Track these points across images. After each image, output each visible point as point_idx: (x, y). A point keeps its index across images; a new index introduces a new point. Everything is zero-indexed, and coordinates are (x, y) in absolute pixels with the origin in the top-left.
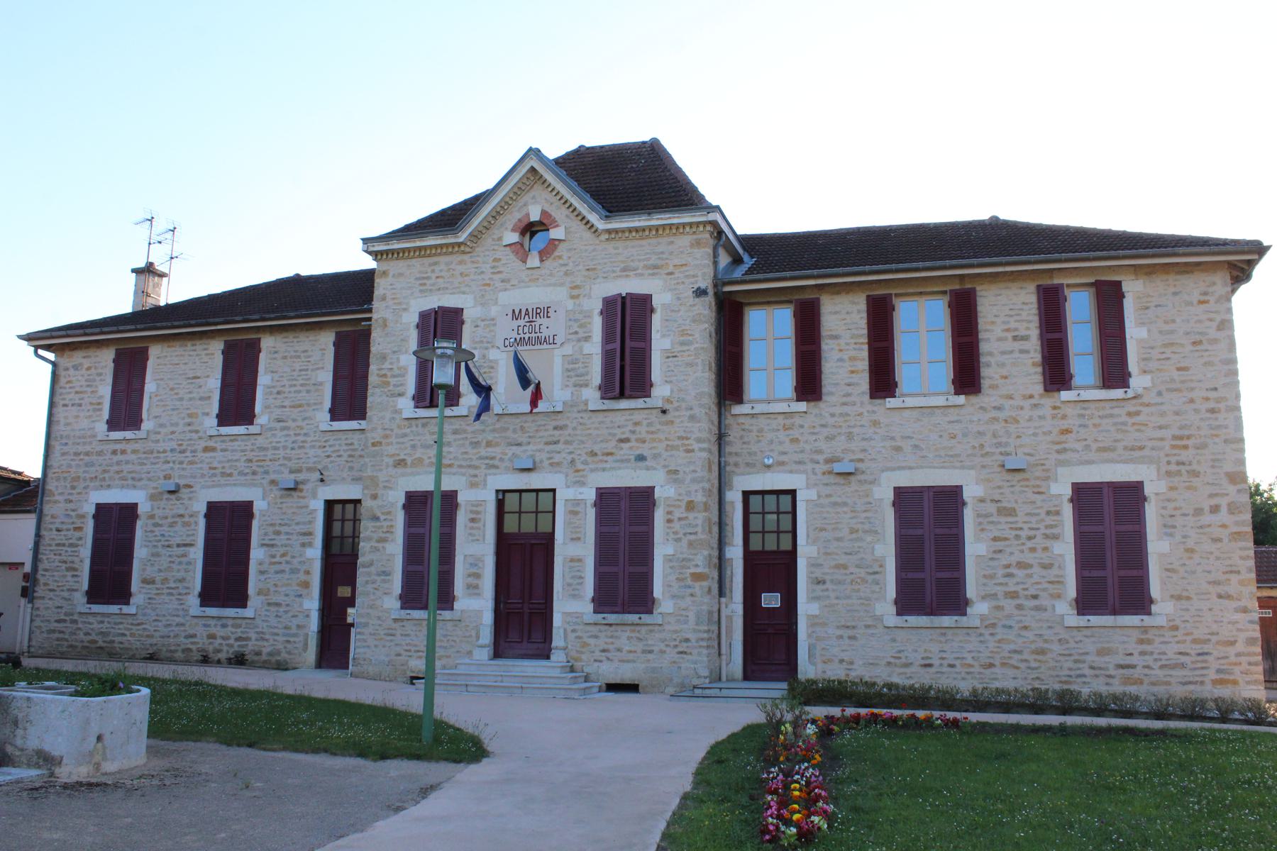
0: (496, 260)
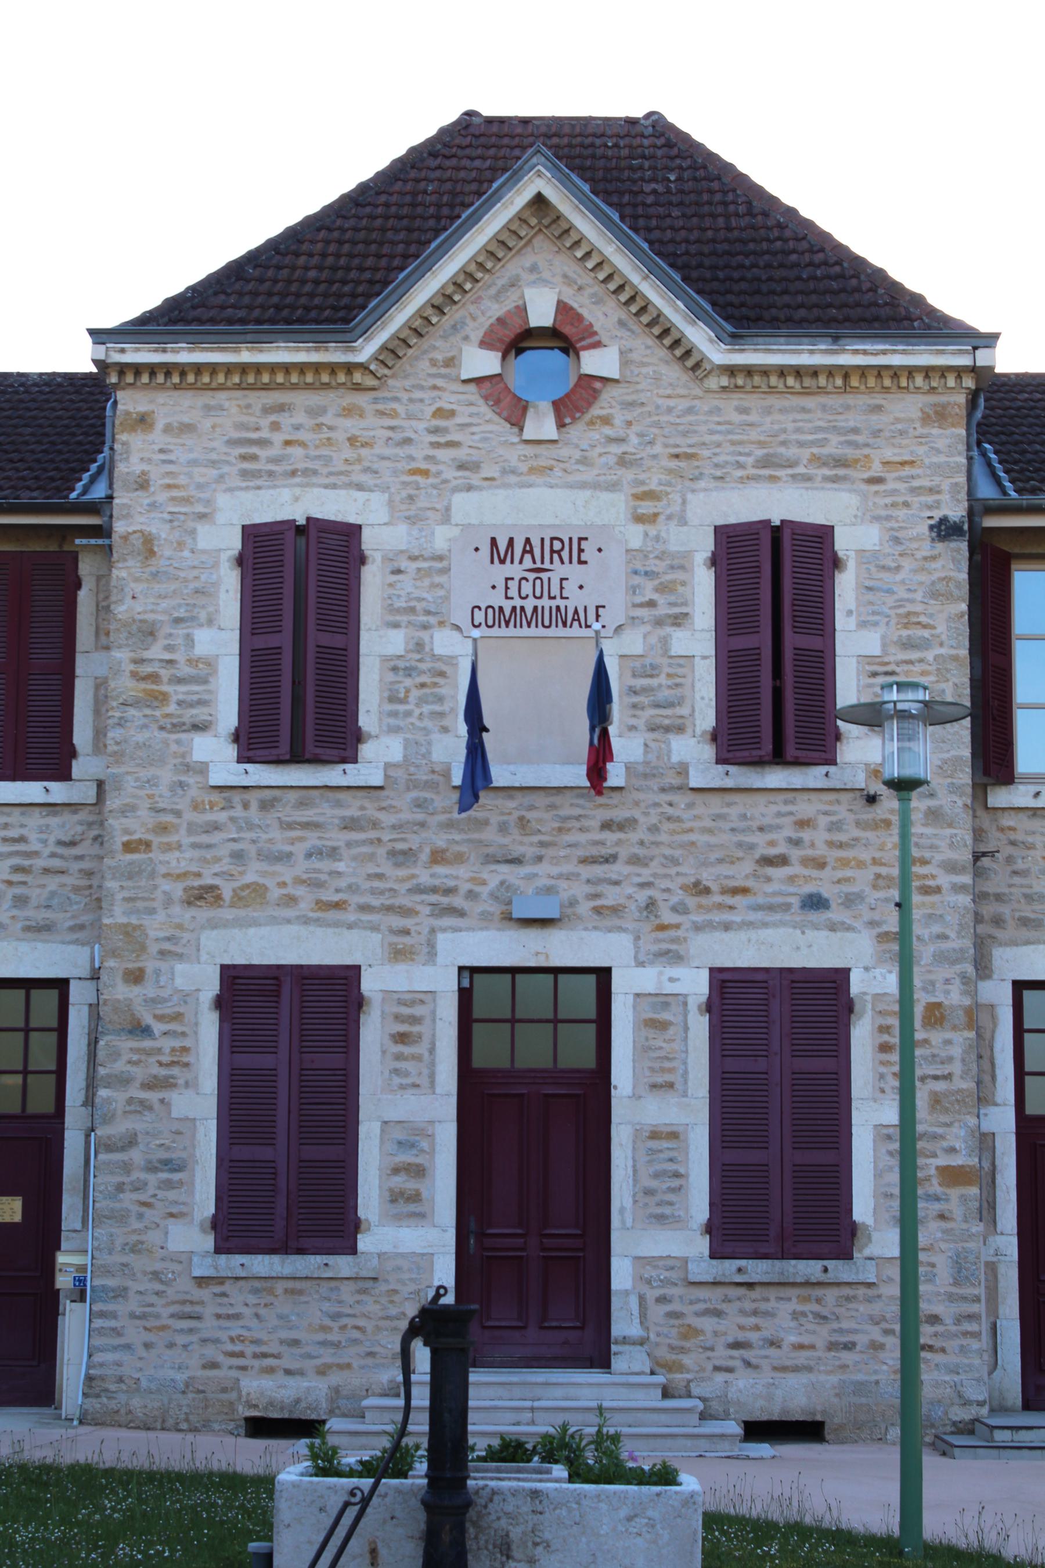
0: (439, 413)
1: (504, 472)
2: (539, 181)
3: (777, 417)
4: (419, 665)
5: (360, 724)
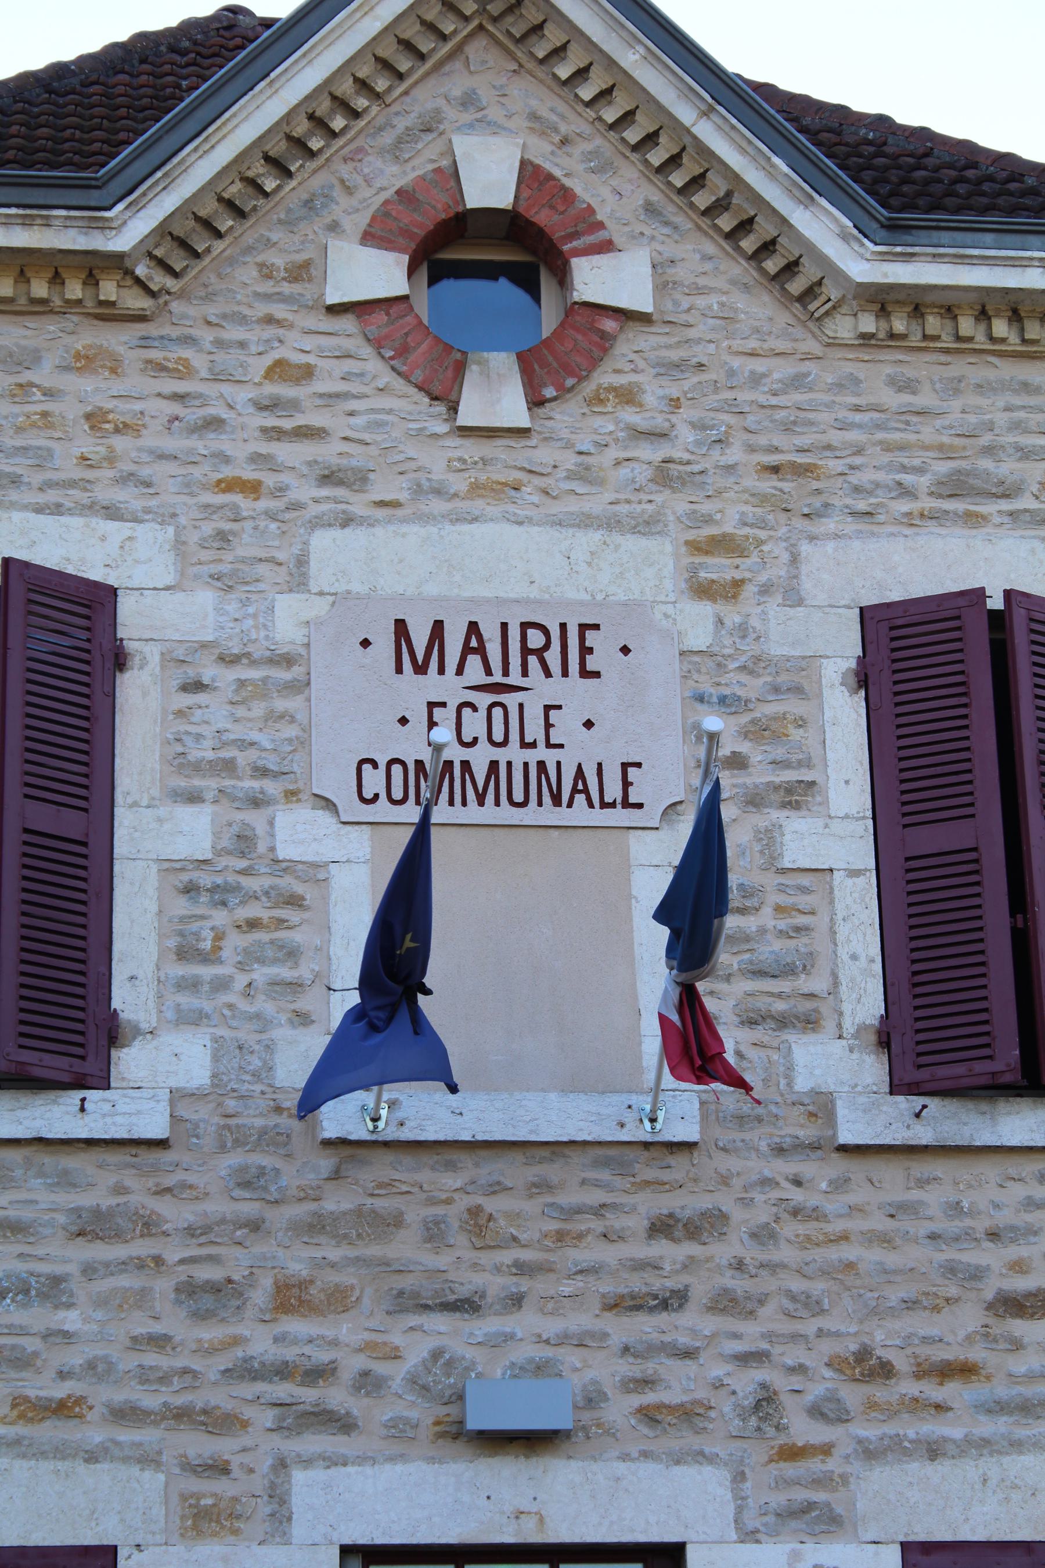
0: (279, 370)
1: (418, 490)
3: (974, 400)
4: (246, 882)
5: (116, 1004)
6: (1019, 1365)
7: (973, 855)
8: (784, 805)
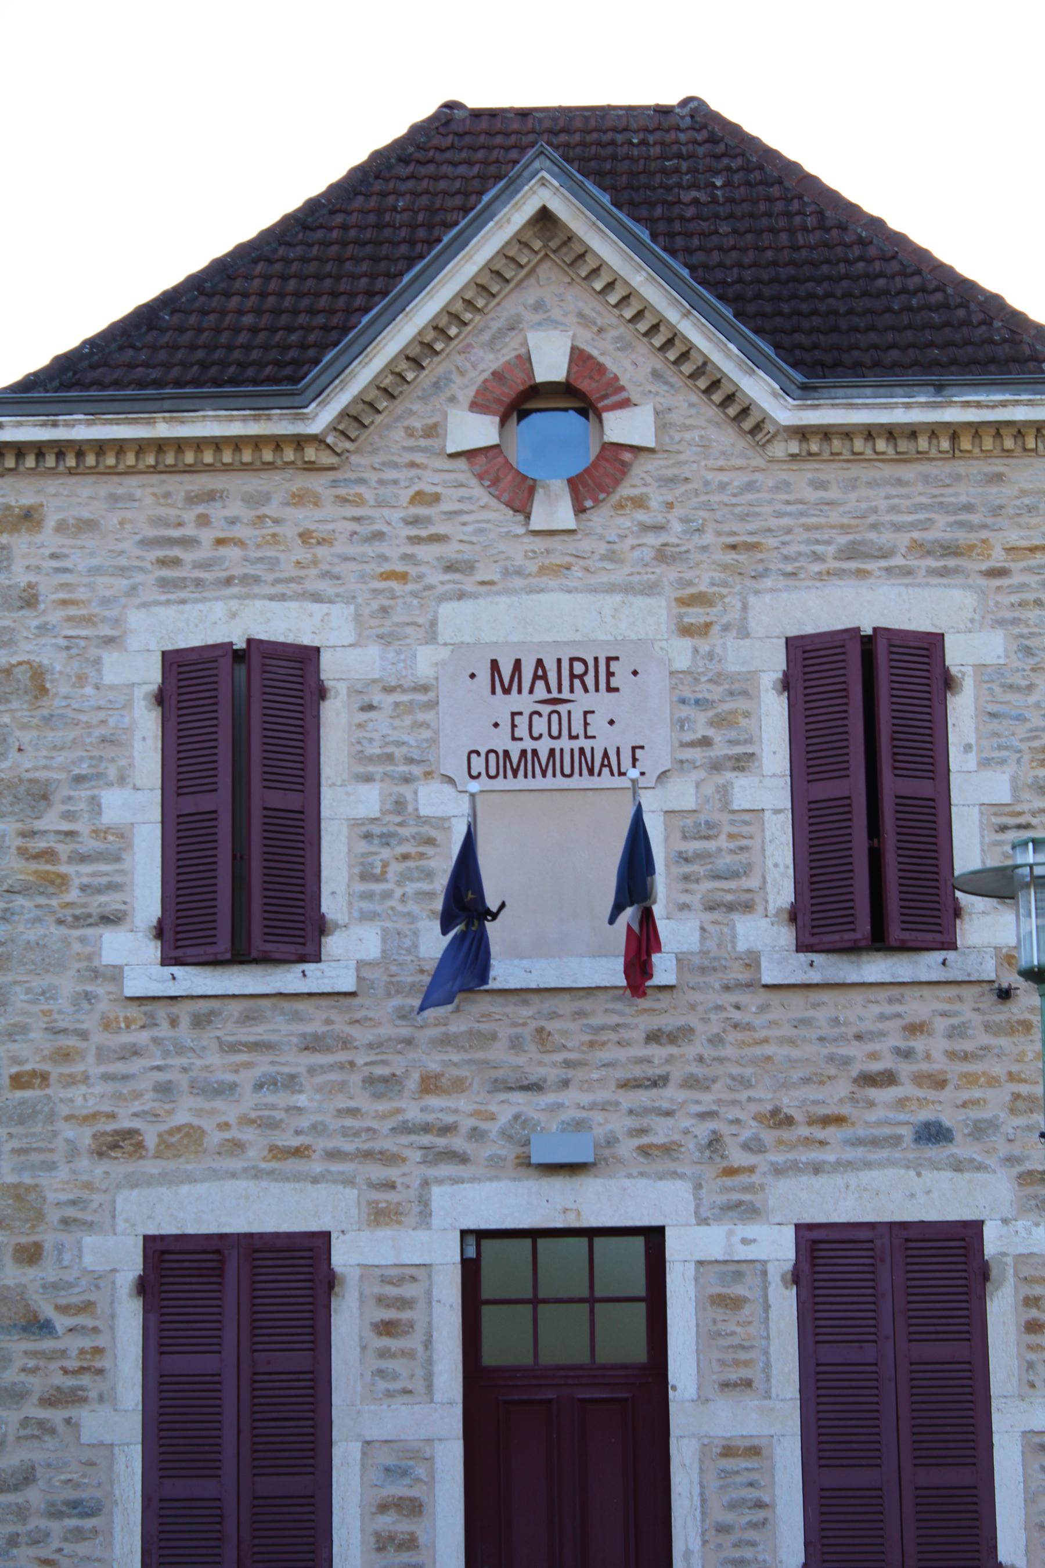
0: (419, 498)
1: (506, 573)
2: (543, 191)
3: (865, 492)
4: (401, 831)
5: (324, 909)
6: (872, 1116)
7: (847, 802)
8: (736, 769)
